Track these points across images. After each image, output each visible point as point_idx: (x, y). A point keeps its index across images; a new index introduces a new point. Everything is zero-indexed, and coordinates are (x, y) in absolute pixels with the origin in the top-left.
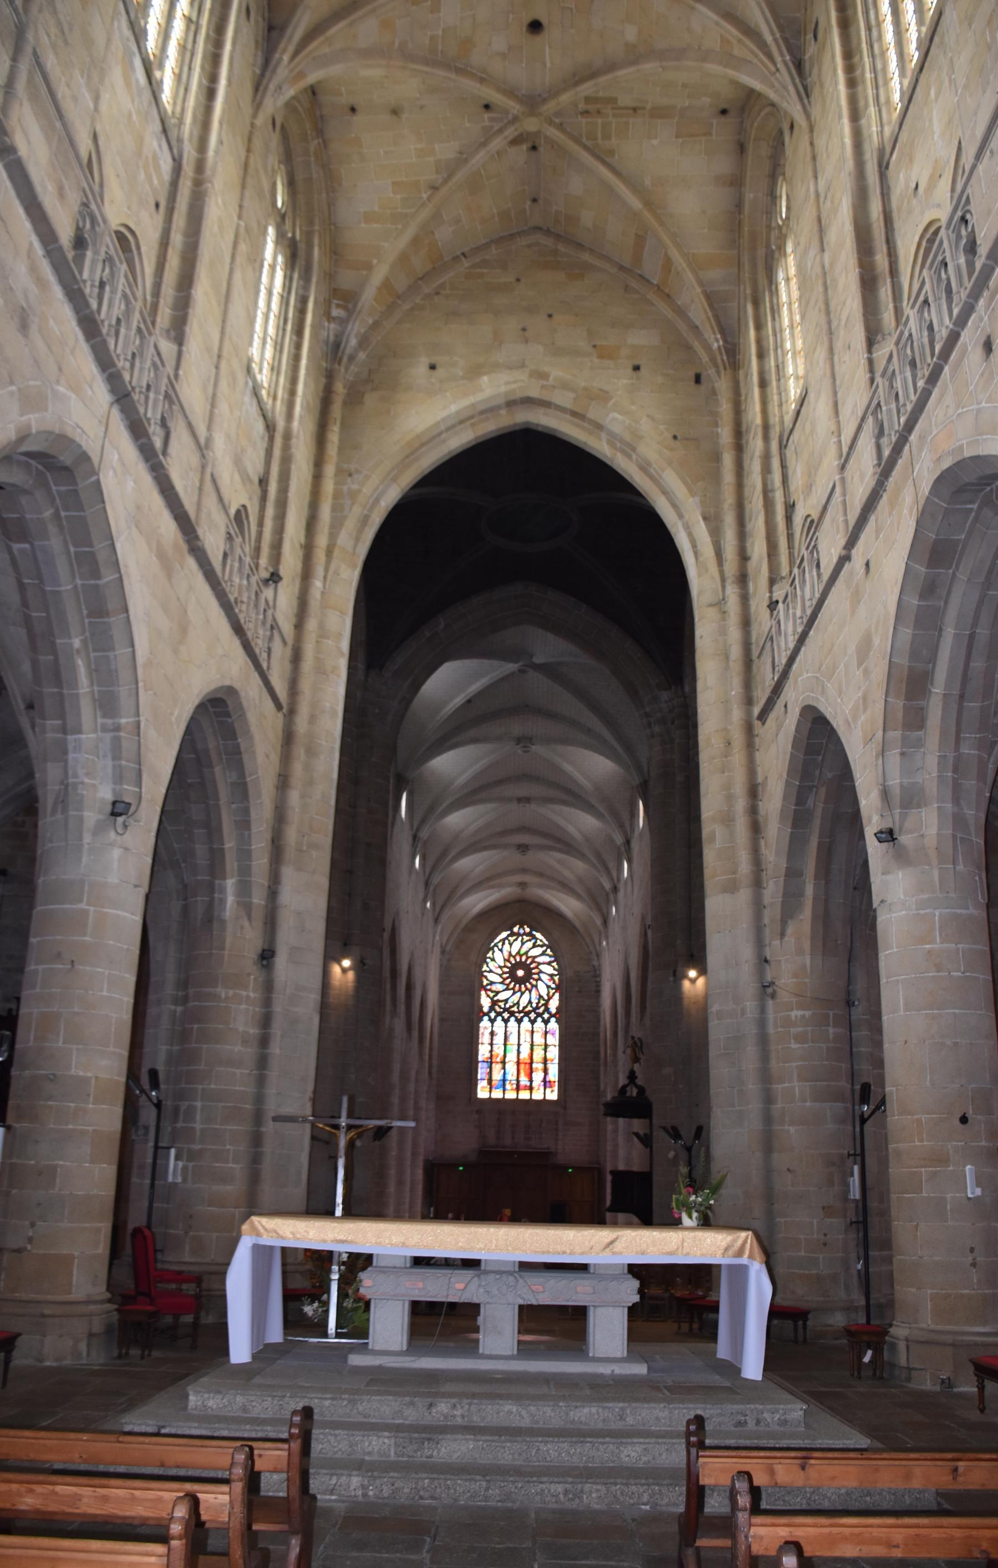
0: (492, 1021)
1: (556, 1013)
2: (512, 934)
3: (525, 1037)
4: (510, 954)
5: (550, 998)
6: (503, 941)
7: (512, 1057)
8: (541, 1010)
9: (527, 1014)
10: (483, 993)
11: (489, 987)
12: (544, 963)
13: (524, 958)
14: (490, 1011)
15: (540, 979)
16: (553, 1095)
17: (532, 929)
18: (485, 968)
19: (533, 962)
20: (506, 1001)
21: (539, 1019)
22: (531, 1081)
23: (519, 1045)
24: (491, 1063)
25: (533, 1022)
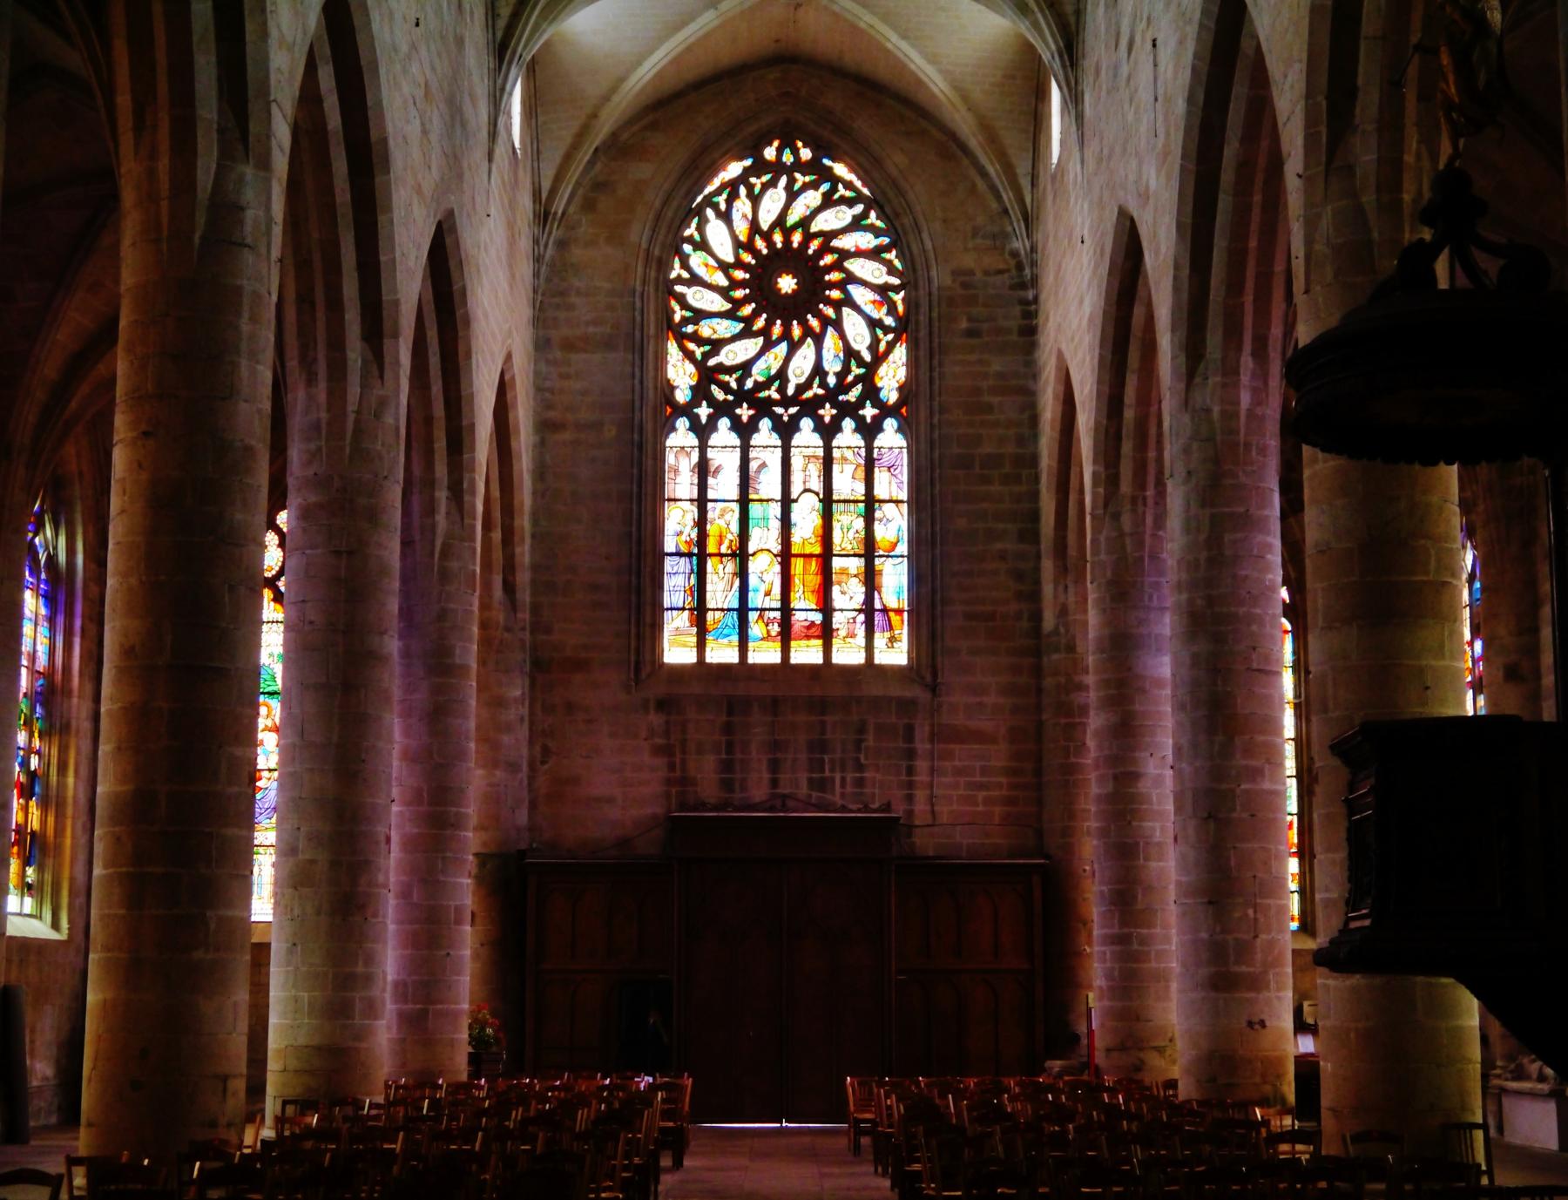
0: (703, 432)
1: (901, 402)
2: (760, 167)
3: (806, 475)
4: (754, 227)
5: (879, 358)
6: (732, 187)
7: (765, 537)
8: (853, 395)
9: (810, 408)
10: (672, 348)
11: (690, 329)
12: (859, 253)
13: (797, 238)
14: (694, 403)
15: (849, 302)
16: (894, 653)
17: (820, 149)
18: (677, 271)
19: (826, 249)
20: (746, 367)
21: (848, 424)
22: (826, 608)
23: (787, 501)
24: (702, 557)
25: (828, 432)
